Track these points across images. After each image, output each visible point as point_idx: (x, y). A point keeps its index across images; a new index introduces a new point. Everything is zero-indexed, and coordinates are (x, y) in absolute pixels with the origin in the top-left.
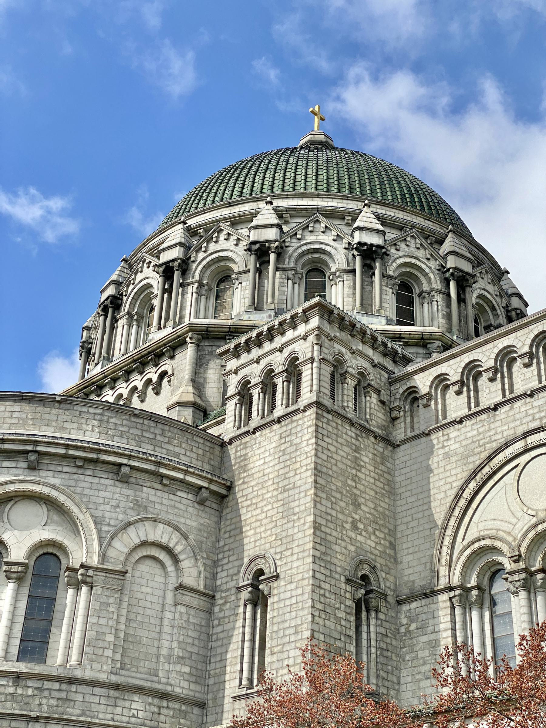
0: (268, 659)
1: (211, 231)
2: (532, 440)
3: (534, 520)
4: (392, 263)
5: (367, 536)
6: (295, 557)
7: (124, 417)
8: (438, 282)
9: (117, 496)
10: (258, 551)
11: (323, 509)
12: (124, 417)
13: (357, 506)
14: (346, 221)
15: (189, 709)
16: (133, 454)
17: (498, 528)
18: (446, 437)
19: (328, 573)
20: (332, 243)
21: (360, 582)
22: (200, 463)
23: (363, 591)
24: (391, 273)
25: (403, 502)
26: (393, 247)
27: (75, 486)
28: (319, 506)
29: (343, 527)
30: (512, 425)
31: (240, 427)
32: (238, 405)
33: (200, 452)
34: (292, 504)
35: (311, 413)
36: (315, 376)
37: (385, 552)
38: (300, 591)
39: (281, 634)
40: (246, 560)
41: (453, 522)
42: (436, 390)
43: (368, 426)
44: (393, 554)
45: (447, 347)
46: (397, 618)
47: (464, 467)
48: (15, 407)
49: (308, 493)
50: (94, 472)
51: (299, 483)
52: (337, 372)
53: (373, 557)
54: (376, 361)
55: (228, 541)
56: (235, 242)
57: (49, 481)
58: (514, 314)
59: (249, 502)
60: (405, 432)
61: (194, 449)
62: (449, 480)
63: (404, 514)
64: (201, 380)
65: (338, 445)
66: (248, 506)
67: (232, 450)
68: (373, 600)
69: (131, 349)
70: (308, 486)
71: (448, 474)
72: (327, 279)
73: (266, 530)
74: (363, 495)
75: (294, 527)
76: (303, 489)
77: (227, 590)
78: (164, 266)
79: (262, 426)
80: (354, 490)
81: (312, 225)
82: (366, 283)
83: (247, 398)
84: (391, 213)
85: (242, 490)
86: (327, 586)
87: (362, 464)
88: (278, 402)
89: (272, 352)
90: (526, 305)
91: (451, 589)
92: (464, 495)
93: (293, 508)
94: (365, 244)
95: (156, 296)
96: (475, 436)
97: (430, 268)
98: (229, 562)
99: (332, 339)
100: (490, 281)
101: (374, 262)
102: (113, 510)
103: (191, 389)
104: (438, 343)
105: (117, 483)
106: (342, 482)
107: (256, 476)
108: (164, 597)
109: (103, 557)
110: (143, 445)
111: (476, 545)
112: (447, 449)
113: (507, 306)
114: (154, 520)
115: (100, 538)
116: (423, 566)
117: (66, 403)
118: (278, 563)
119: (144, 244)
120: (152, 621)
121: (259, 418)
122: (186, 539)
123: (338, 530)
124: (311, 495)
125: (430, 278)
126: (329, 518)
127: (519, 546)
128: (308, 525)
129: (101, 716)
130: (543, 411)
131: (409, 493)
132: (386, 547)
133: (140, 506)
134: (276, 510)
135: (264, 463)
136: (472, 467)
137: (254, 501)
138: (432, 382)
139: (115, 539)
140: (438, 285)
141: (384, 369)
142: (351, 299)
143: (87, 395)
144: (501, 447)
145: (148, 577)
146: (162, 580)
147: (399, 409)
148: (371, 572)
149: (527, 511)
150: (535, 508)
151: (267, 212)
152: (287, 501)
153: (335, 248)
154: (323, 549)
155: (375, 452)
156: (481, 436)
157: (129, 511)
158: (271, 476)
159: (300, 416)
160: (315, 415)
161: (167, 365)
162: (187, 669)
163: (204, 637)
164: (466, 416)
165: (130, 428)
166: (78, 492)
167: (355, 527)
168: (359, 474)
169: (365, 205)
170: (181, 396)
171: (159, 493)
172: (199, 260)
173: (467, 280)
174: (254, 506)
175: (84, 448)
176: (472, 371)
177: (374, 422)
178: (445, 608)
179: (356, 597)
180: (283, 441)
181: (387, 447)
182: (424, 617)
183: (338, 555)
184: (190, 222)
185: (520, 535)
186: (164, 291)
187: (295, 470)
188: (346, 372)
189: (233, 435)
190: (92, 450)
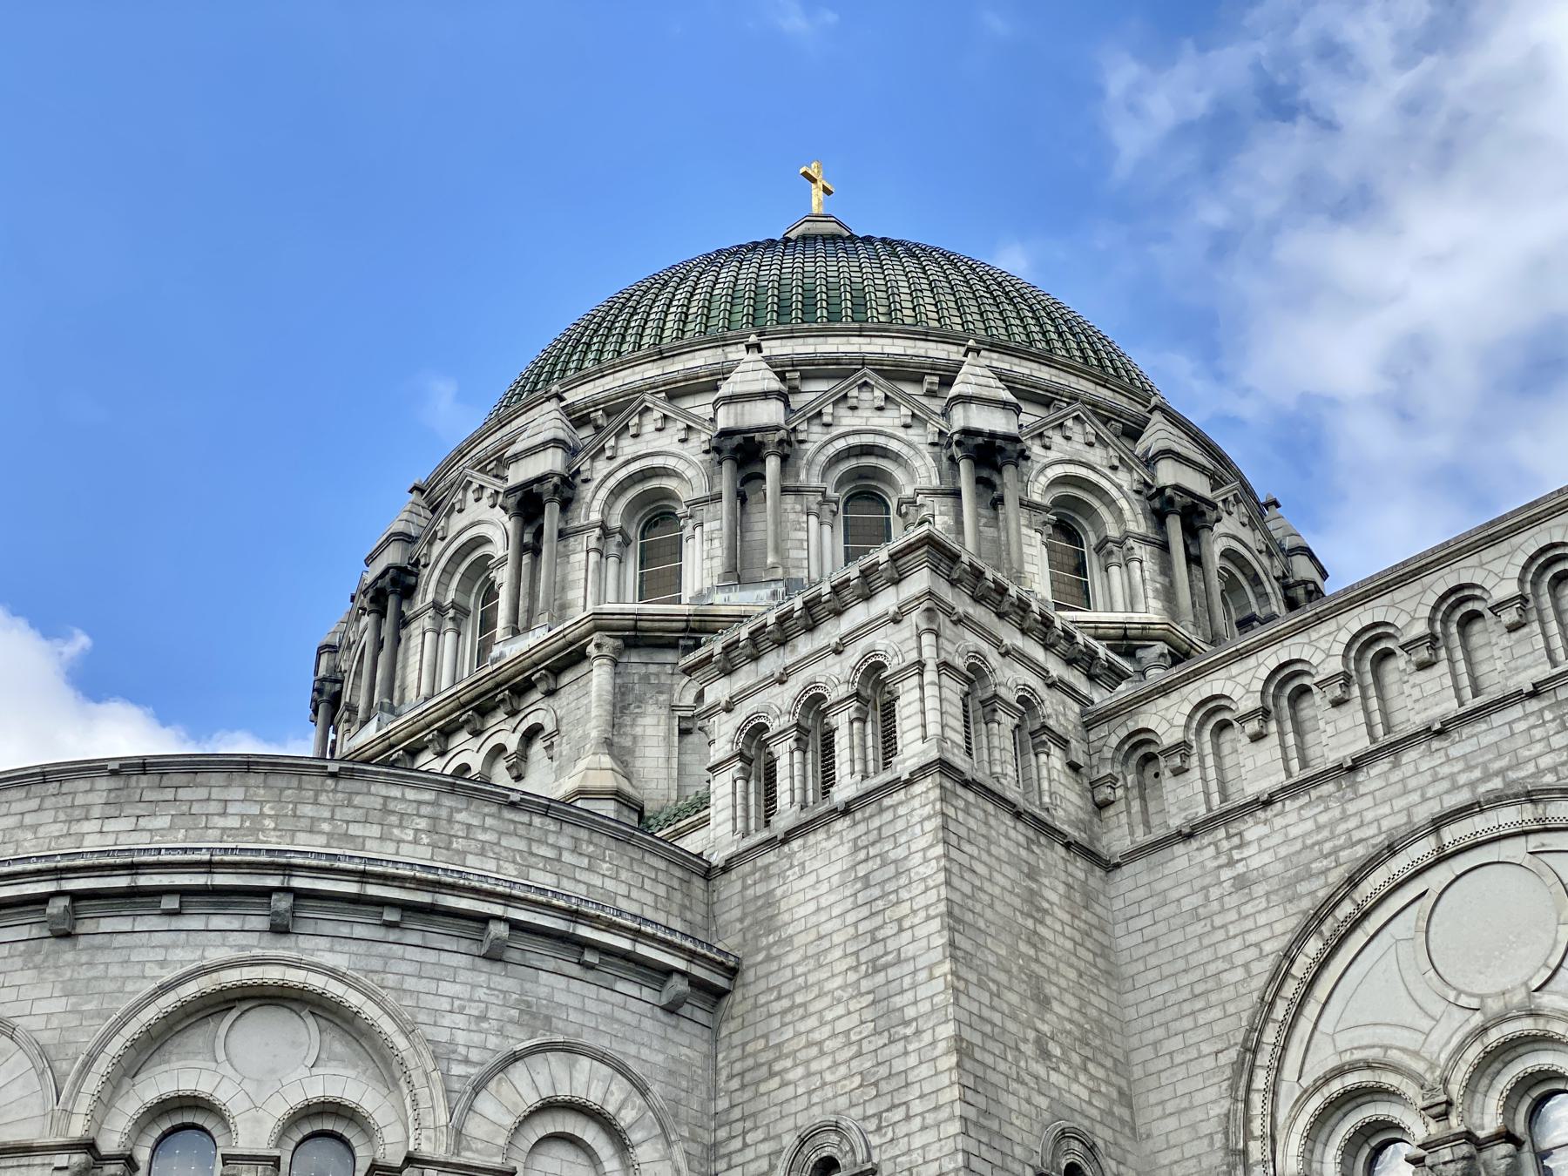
2: (1453, 834)
3: (1477, 1019)
6: (916, 1123)
7: (486, 810)
8: (1141, 517)
9: (480, 993)
10: (818, 1116)
11: (974, 1008)
13: (1044, 1002)
14: (926, 386)
16: (515, 892)
17: (1386, 1042)
18: (1236, 840)
19: (996, 1158)
20: (901, 433)
24: (1036, 498)
25: (1142, 995)
28: (963, 1000)
29: (1018, 1049)
30: (1400, 803)
31: (746, 834)
32: (740, 783)
33: (662, 891)
35: (927, 788)
36: (931, 703)
41: (1270, 1035)
42: (1199, 732)
43: (1049, 820)
44: (1127, 1118)
48: (232, 790)
49: (938, 972)
50: (424, 938)
51: (910, 951)
53: (1087, 1123)
56: (682, 435)
58: (1300, 592)
59: (786, 1003)
60: (1132, 833)
61: (648, 884)
62: (1252, 938)
63: (1147, 1022)
64: (627, 742)
65: (993, 862)
66: (784, 1012)
70: (936, 955)
71: (1249, 924)
73: (835, 1065)
74: (1054, 978)
75: (906, 1053)
76: (922, 962)
78: (519, 494)
79: (807, 824)
80: (1034, 966)
81: (854, 393)
82: (983, 521)
83: (759, 767)
84: (1023, 368)
85: (767, 975)
87: (1046, 905)
89: (817, 656)
92: (1294, 971)
93: (902, 1009)
94: (979, 433)
95: (503, 561)
96: (1309, 833)
97: (1119, 488)
101: (1000, 472)
102: (473, 1027)
103: (606, 761)
104: (1161, 647)
105: (480, 962)
107: (798, 941)
110: (533, 874)
111: (1336, 1086)
112: (1240, 868)
113: (1285, 576)
114: (569, 1049)
115: (448, 1091)
116: (1206, 1141)
119: (460, 452)
121: (797, 807)
123: (1010, 1058)
125: (1121, 510)
126: (988, 1029)
127: (1445, 1082)
128: (942, 1046)
130: (1475, 767)
132: (1113, 1102)
133: (534, 1016)
135: (818, 910)
136: (1306, 904)
137: (799, 999)
138: (1190, 717)
139: (483, 1094)
140: (1137, 523)
141: (1071, 691)
143: (413, 752)
144: (1379, 854)
147: (1112, 781)
148: (1086, 1160)
150: (1476, 991)
152: (883, 993)
153: (910, 445)
154: (981, 1101)
155: (1070, 880)
156: (1325, 833)
158: (837, 939)
159: (901, 795)
160: (938, 791)
164: (1283, 789)
165: (501, 834)
166: (391, 984)
167: (1045, 1054)
168: (1041, 929)
169: (969, 350)
170: (585, 777)
172: (598, 477)
173: (1203, 514)
174: (801, 1011)
175: (403, 879)
176: (1290, 685)
177: (1061, 813)
180: (862, 855)
183: (1014, 1116)
184: (571, 397)
185: (1444, 1056)
186: (523, 548)
187: (900, 920)
188: (996, 696)
190: (421, 884)
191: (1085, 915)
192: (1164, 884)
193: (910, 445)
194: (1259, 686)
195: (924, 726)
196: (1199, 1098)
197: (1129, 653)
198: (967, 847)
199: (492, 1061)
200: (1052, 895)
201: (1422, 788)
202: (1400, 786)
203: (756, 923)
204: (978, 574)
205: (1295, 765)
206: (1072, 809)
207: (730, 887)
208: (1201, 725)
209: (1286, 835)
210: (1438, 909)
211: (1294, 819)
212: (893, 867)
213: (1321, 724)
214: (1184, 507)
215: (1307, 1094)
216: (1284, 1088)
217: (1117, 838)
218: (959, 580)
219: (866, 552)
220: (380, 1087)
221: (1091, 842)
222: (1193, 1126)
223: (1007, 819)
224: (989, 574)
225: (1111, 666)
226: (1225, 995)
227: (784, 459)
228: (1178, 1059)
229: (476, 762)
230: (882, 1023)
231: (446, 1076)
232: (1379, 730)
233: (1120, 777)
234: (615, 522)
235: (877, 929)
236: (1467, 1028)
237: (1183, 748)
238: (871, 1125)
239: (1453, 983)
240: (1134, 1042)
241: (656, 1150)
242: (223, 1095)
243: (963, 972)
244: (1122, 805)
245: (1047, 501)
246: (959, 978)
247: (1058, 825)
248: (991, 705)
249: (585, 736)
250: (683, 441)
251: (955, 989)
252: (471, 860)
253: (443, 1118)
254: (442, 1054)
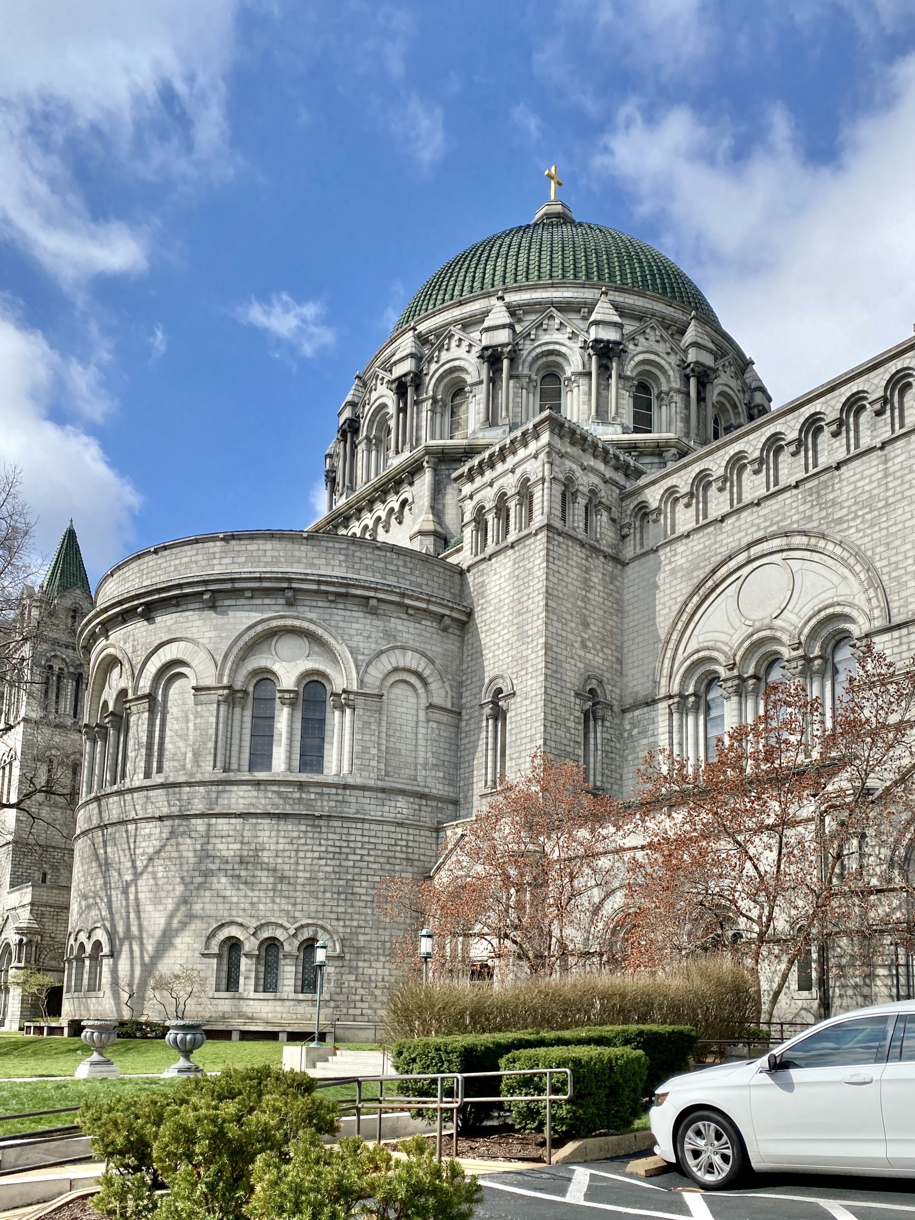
11: (554, 630)
22: (441, 592)
28: (550, 628)
35: (542, 536)
40: (487, 681)
51: (532, 607)
52: (567, 491)
67: (470, 577)
70: (540, 609)
76: (535, 612)
88: (512, 527)
109: (361, 682)
112: (673, 565)
115: (357, 666)
118: (515, 682)
120: (409, 735)
136: (696, 581)
141: (615, 483)
142: (586, 407)
154: (554, 667)
157: (380, 641)
159: (532, 540)
161: (407, 492)
162: (441, 774)
189: (471, 562)
190: (341, 585)
194: (690, 481)
196: (646, 661)
198: (557, 562)
201: (746, 530)
222: (643, 672)
223: (578, 548)
238: (514, 676)
242: (275, 668)
243: (551, 616)
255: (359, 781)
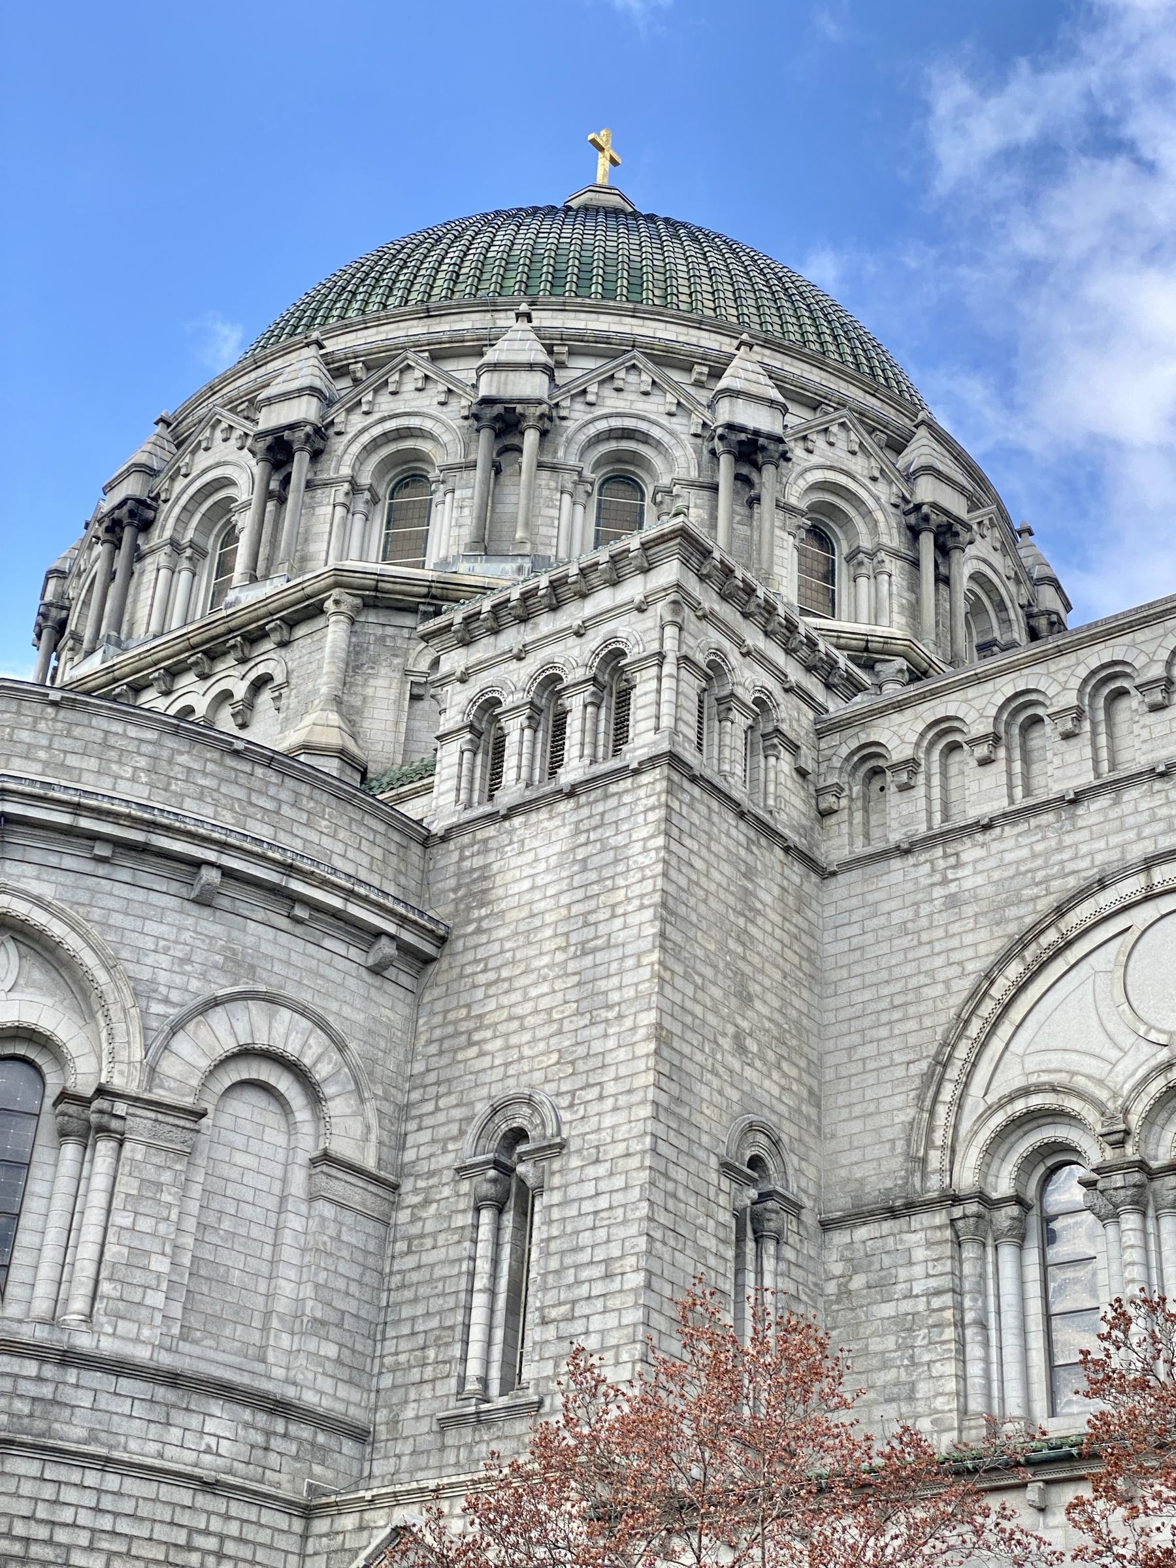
0: (534, 1334)
1: (381, 366)
4: (797, 478)
5: (764, 1070)
6: (609, 1103)
7: (209, 755)
8: (895, 532)
9: (186, 936)
10: (513, 1087)
11: (678, 998)
12: (209, 755)
13: (746, 999)
14: (694, 376)
15: (333, 1443)
16: (230, 840)
17: (1073, 1068)
18: (952, 861)
20: (664, 420)
21: (749, 1171)
23: (753, 1193)
24: (793, 501)
25: (844, 1001)
26: (800, 444)
27: (90, 905)
28: (668, 990)
29: (716, 1043)
30: (1115, 840)
31: (469, 805)
32: (467, 755)
33: (378, 853)
34: (604, 982)
37: (799, 1111)
38: (619, 1182)
39: (569, 1276)
41: (962, 1051)
42: (928, 751)
43: (772, 823)
44: (815, 1117)
45: (917, 674)
46: (819, 1260)
47: (995, 928)
49: (646, 960)
50: (134, 876)
51: (621, 936)
53: (775, 1118)
54: (792, 678)
55: (434, 1062)
56: (442, 398)
57: (29, 888)
58: (1042, 623)
59: (492, 976)
60: (851, 844)
61: (365, 845)
62: (956, 956)
63: (844, 1028)
64: (357, 702)
65: (712, 859)
66: (488, 985)
68: (773, 1216)
69: (198, 616)
70: (645, 944)
71: (955, 942)
72: (648, 501)
73: (534, 1041)
74: (759, 977)
75: (606, 1036)
76: (631, 949)
77: (431, 1174)
78: (269, 439)
80: (741, 964)
81: (621, 374)
82: (738, 518)
85: (475, 947)
86: (680, 1175)
87: (759, 906)
89: (557, 636)
90: (1068, 607)
91: (956, 1200)
93: (606, 993)
94: (742, 429)
95: (247, 505)
96: (1024, 860)
97: (877, 499)
98: (438, 1109)
99: (705, 617)
100: (998, 545)
101: (759, 470)
102: (176, 969)
103: (334, 718)
104: (901, 663)
105: (189, 906)
106: (717, 942)
107: (509, 916)
108: (284, 1180)
110: (250, 823)
111: (1020, 1106)
112: (953, 888)
113: (1030, 605)
114: (271, 999)
115: (145, 1029)
116: (888, 1146)
117: (73, 708)
119: (211, 388)
120: (255, 1232)
121: (522, 785)
122: (340, 1050)
123: (707, 1050)
124: (652, 964)
125: (876, 522)
126: (689, 1020)
127: (1126, 1111)
128: (641, 1033)
129: (133, 1445)
131: (855, 983)
132: (801, 1100)
133: (238, 964)
134: (560, 995)
135: (533, 888)
136: (1013, 928)
137: (505, 973)
138: (922, 736)
139: (181, 1035)
140: (892, 537)
141: (807, 698)
143: (137, 689)
144: (1089, 887)
145: (249, 1129)
146: (282, 1140)
149: (1147, 1033)
150: (1166, 1028)
151: (519, 335)
152: (588, 975)
153: (672, 433)
154: (674, 1089)
155: (786, 883)
156: (1040, 862)
157: (214, 974)
158: (548, 918)
160: (665, 783)
162: (331, 1350)
163: (370, 1278)
164: (1005, 815)
165: (222, 780)
166: (96, 918)
167: (741, 1049)
169: (742, 343)
170: (311, 732)
171: (283, 938)
172: (352, 431)
174: (506, 985)
175: (118, 815)
176: (1024, 715)
178: (939, 1243)
179: (737, 1204)
180: (582, 838)
181: (808, 876)
182: (887, 1261)
183: (704, 1105)
184: (331, 346)
185: (1128, 1087)
186: (269, 495)
188: (732, 694)
191: (797, 919)
192: (877, 896)
193: (672, 433)
194: (993, 711)
195: (658, 718)
196: (885, 1105)
197: (869, 666)
198: (687, 841)
199: (192, 1004)
200: (767, 896)
202: (1118, 822)
203: (470, 894)
204: (728, 572)
205: (1018, 792)
206: (795, 814)
207: (448, 857)
208: (932, 744)
209: (1002, 860)
210: (1139, 947)
211: (1012, 847)
212: (612, 853)
213: (1049, 755)
214: (939, 526)
215: (991, 1110)
216: (969, 1102)
217: (837, 845)
218: (708, 576)
219: (617, 537)
220: (76, 1017)
221: (810, 849)
223: (731, 818)
224: (739, 574)
225: (850, 678)
226: (923, 1008)
227: (544, 433)
228: (871, 1065)
229: (201, 706)
230: (585, 1004)
231: (145, 1013)
232: (1105, 766)
233: (846, 787)
234: (365, 479)
235: (589, 912)
236: (1153, 1063)
237: (911, 765)
238: (564, 1102)
239: (1146, 1017)
240: (830, 1045)
241: (348, 1106)
243: (670, 962)
244: (844, 815)
245: (803, 505)
246: (666, 968)
247: (780, 828)
248: (727, 702)
249: (316, 691)
250: (442, 404)
251: (661, 978)
252: (188, 803)
253: (138, 1054)
254: (142, 992)
255: (108, 1346)
